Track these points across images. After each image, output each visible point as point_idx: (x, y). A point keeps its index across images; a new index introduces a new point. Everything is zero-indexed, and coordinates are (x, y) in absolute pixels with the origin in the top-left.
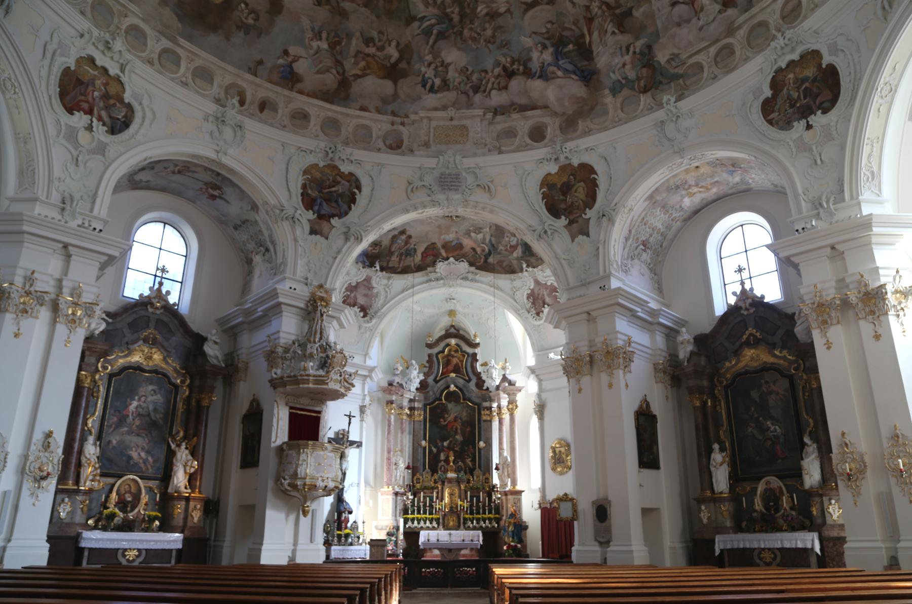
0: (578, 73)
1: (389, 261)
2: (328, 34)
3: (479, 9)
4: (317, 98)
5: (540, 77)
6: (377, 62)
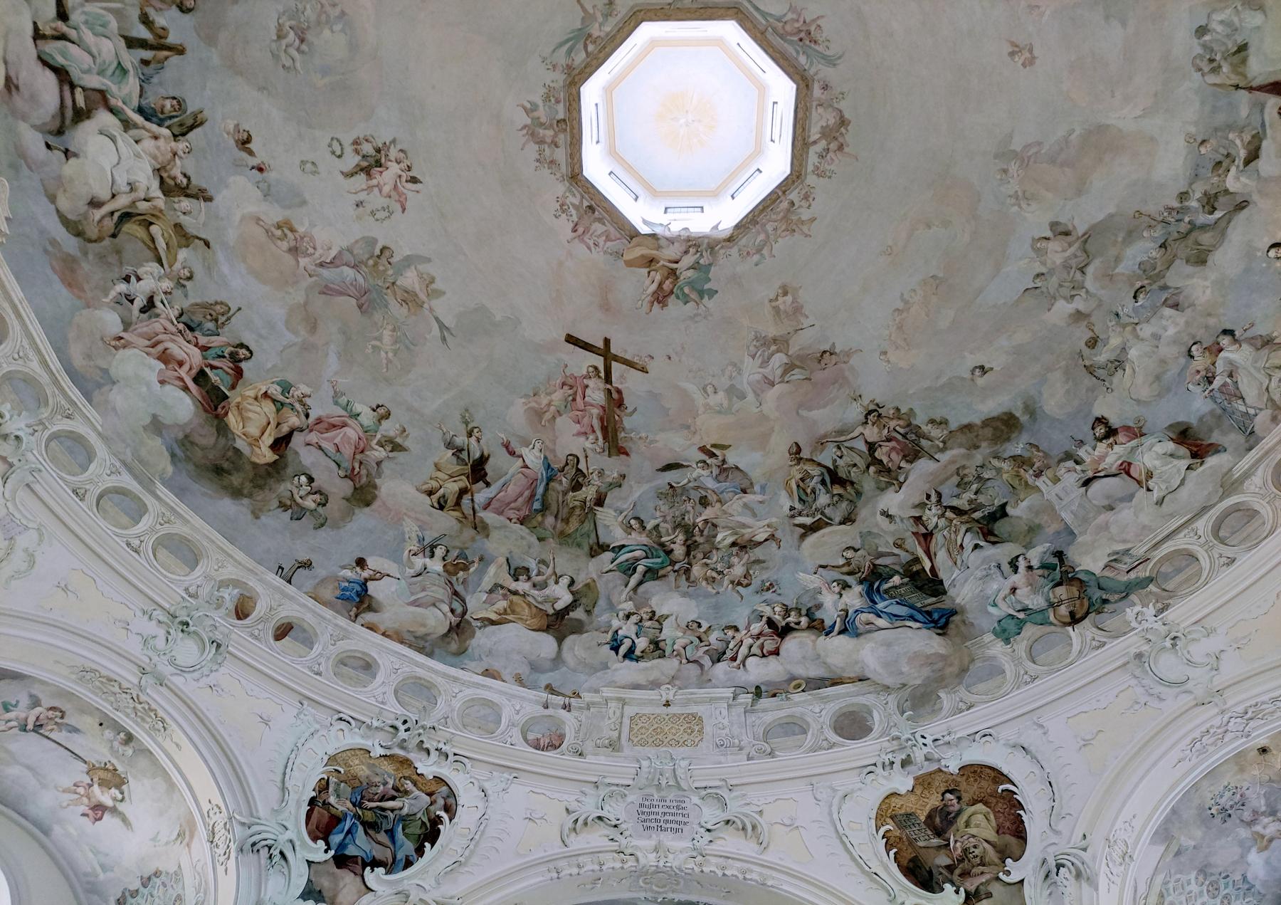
0: (919, 617)
2: (448, 551)
3: (719, 537)
4: (402, 643)
5: (843, 631)
6: (529, 604)
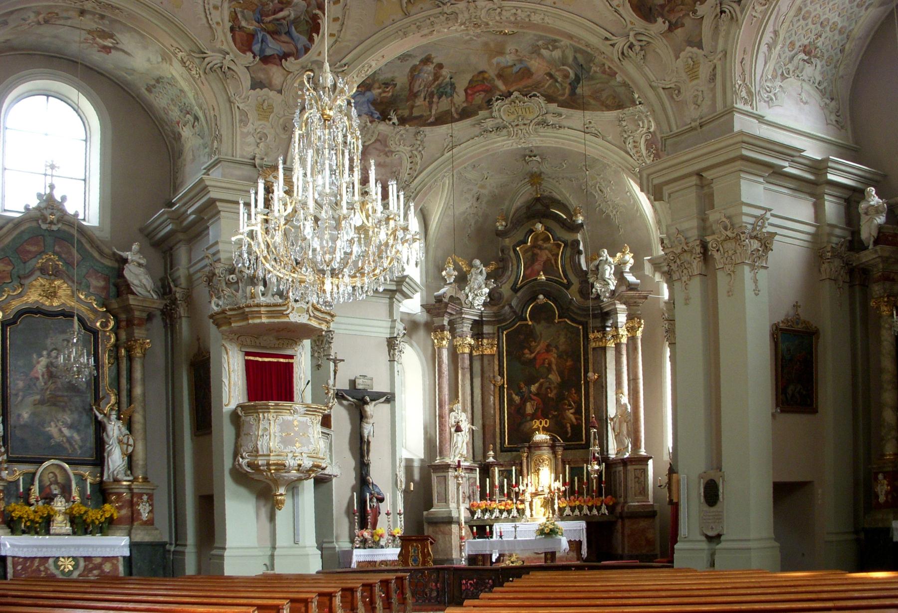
1: (412, 107)
